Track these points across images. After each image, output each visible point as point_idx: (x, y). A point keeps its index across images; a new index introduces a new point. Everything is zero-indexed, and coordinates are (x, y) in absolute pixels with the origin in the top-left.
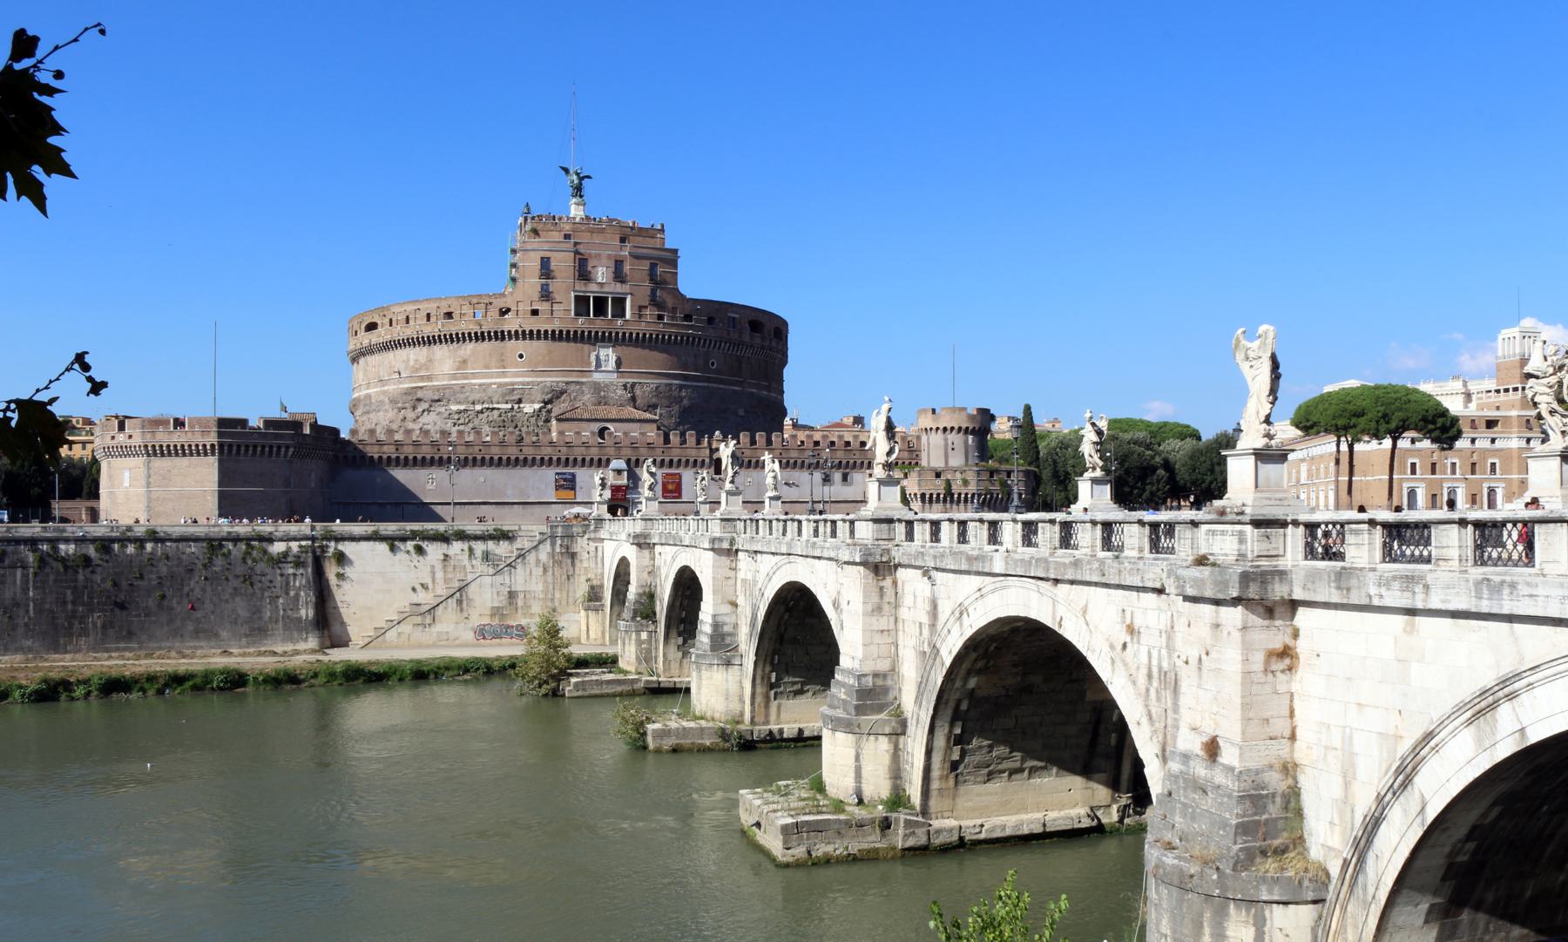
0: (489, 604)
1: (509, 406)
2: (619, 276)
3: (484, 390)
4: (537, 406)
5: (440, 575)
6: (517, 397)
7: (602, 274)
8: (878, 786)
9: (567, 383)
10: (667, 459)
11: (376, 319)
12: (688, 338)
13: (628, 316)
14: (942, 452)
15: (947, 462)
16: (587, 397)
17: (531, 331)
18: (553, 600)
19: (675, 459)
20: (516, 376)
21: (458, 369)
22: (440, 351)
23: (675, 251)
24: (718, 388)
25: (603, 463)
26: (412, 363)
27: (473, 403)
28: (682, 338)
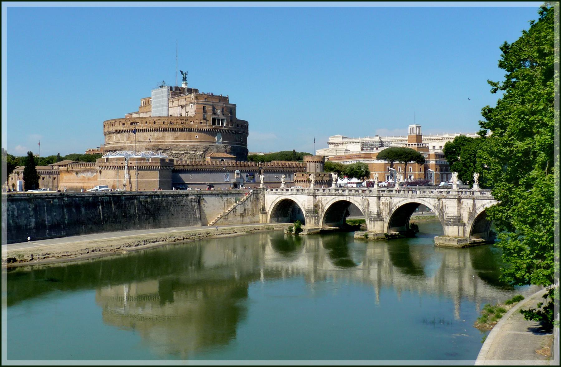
0: (240, 213)
1: (193, 152)
3: (185, 147)
4: (202, 152)
5: (226, 205)
6: (195, 149)
7: (219, 112)
8: (461, 234)
9: (210, 145)
13: (225, 125)
14: (314, 168)
18: (254, 211)
22: (167, 134)
23: (235, 105)
26: (155, 137)
27: (181, 151)
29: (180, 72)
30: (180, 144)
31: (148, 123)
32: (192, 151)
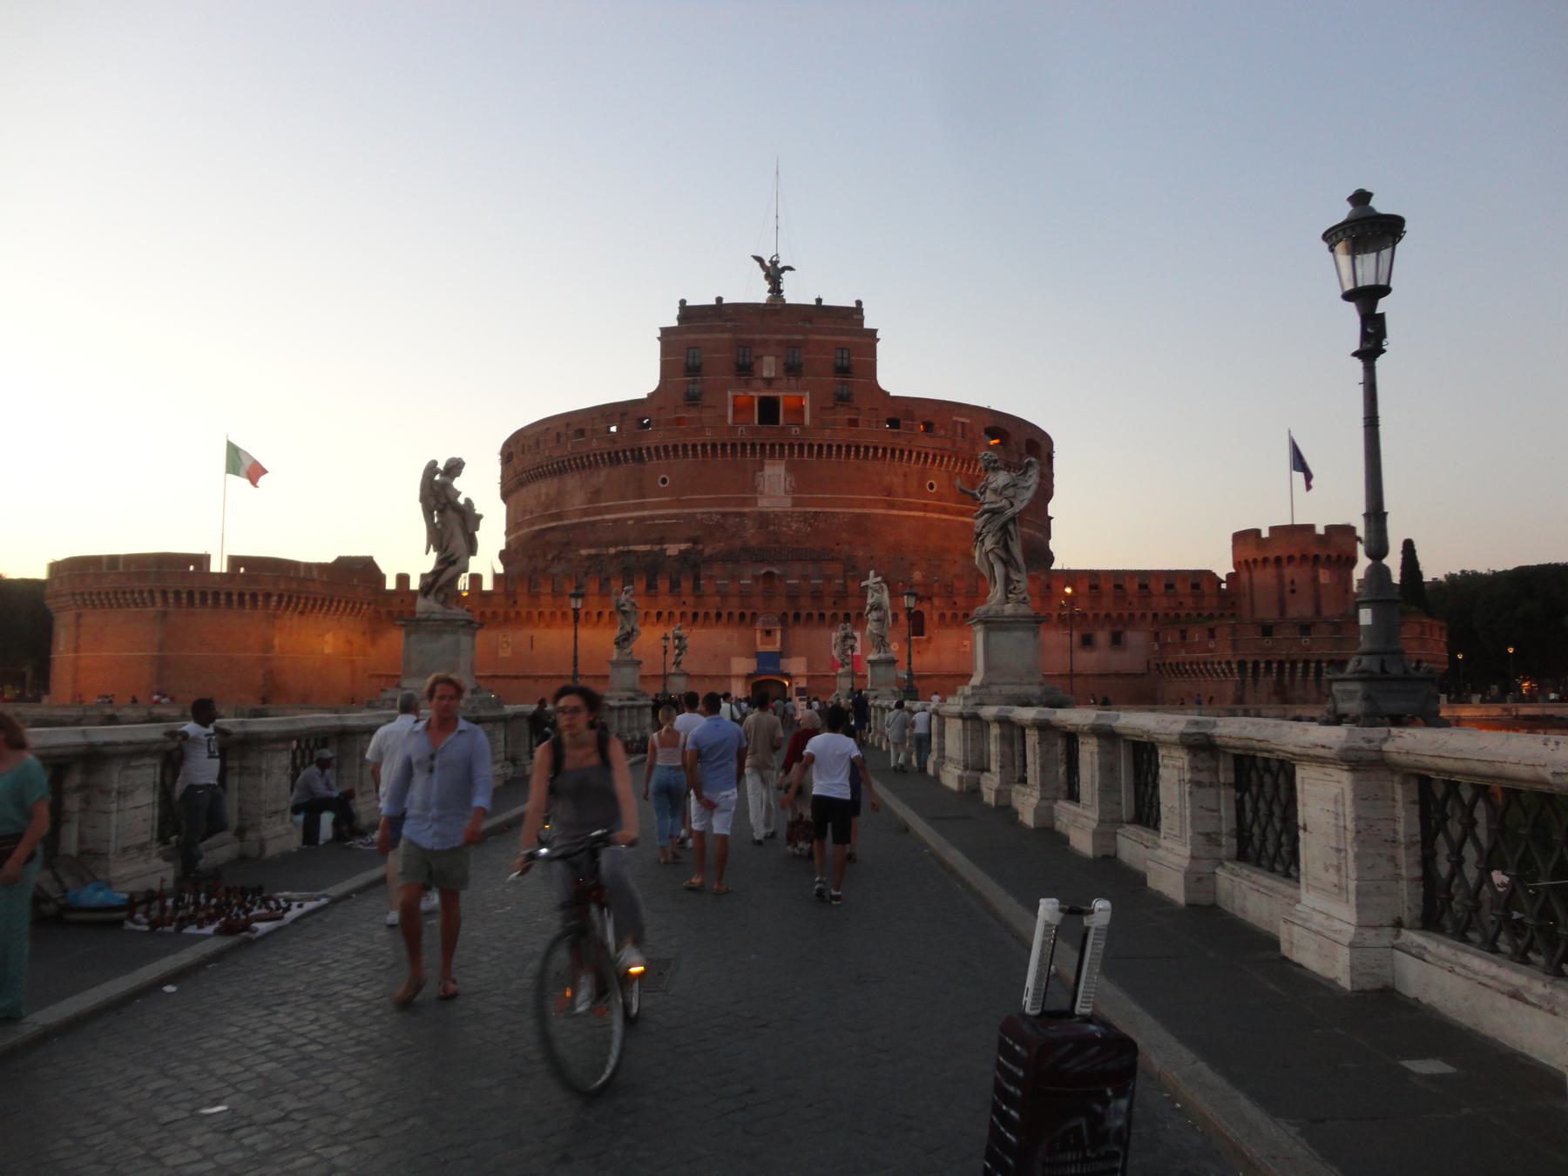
1: (647, 548)
2: (792, 370)
4: (683, 546)
7: (769, 367)
9: (724, 515)
10: (841, 613)
11: (513, 450)
12: (893, 451)
15: (1282, 612)
16: (750, 529)
17: (675, 447)
19: (853, 614)
20: (657, 509)
21: (590, 503)
22: (572, 481)
23: (875, 331)
24: (938, 519)
25: (748, 619)
26: (543, 498)
27: (607, 547)
28: (885, 450)
29: (757, 264)
30: (608, 517)
31: (526, 448)
32: (645, 543)
